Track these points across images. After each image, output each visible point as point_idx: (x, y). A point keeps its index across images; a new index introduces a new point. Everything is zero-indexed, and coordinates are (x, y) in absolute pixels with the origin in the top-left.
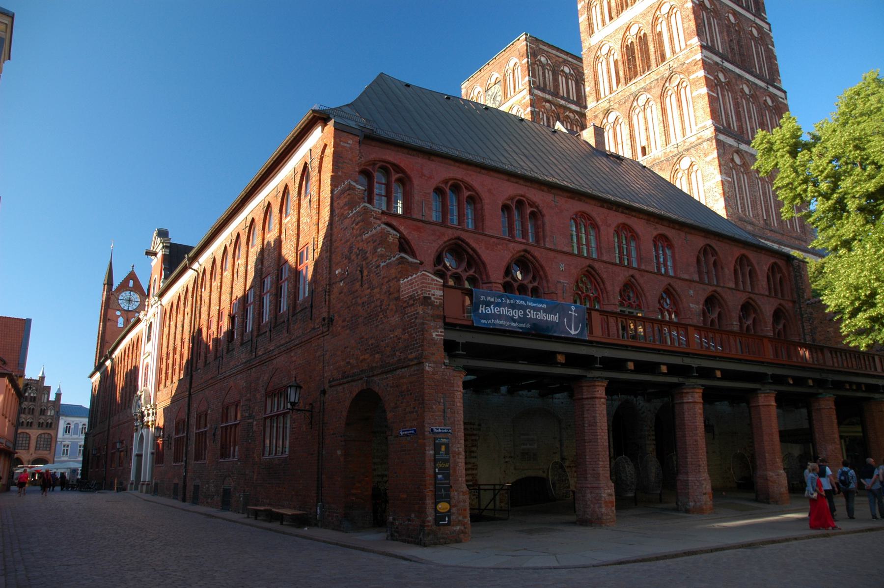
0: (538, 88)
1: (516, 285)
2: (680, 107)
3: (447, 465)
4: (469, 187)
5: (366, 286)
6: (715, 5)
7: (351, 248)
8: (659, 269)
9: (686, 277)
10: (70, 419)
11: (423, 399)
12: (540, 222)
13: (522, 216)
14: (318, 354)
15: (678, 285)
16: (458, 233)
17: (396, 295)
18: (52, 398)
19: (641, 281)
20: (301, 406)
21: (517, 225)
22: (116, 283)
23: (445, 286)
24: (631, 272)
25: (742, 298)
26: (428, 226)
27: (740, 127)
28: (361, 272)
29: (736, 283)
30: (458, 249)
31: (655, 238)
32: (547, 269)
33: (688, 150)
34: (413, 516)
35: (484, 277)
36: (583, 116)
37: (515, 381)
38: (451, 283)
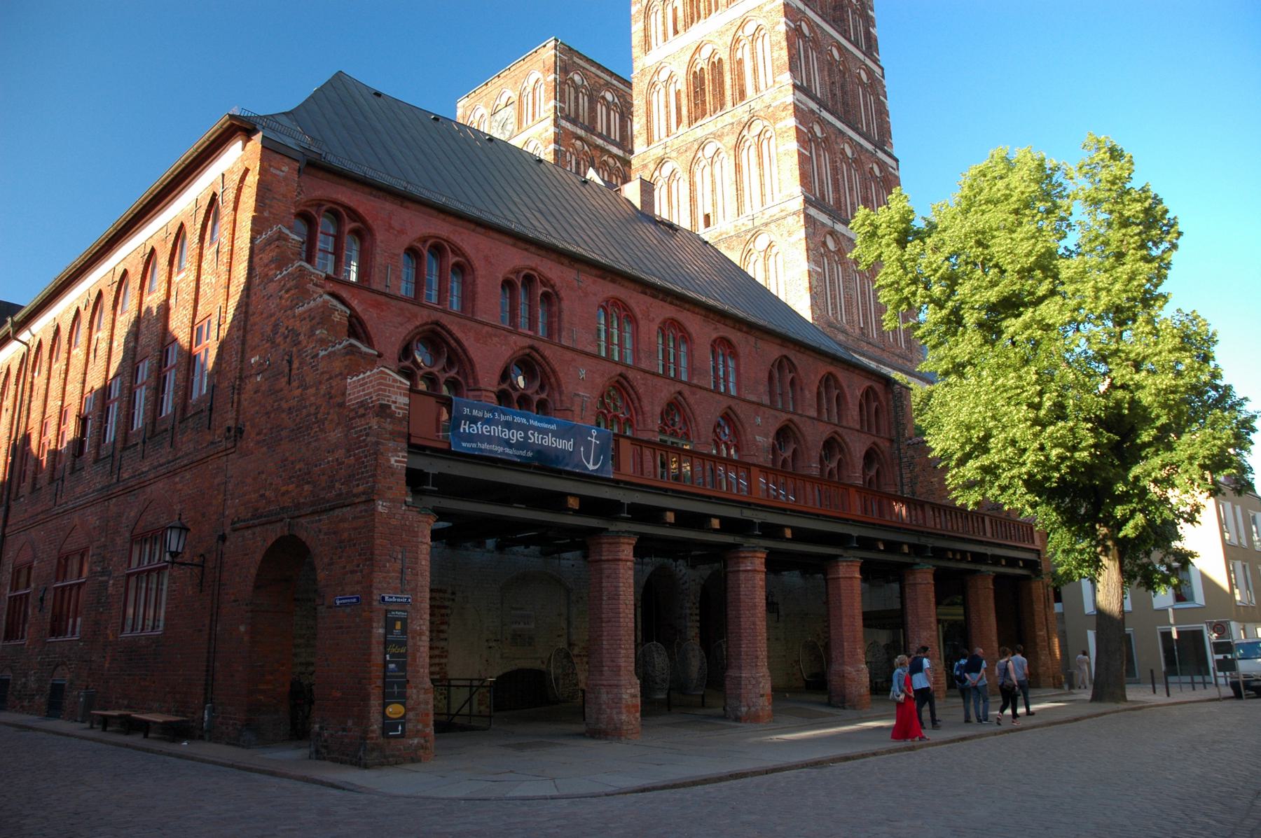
0: (567, 118)
1: (515, 395)
2: (761, 165)
3: (403, 650)
4: (457, 251)
5: (295, 384)
6: (815, 33)
7: (276, 326)
8: (717, 385)
9: (753, 398)
11: (372, 554)
12: (555, 309)
15: (742, 410)
16: (436, 316)
17: (339, 400)
19: (692, 400)
20: (187, 557)
21: (523, 310)
23: (413, 390)
24: (678, 387)
25: (824, 432)
26: (394, 302)
27: (838, 201)
28: (290, 362)
29: (819, 411)
30: (435, 338)
31: (714, 341)
32: (561, 375)
33: (766, 224)
34: (350, 723)
35: (471, 381)
36: (627, 163)
37: (507, 533)
38: (422, 386)
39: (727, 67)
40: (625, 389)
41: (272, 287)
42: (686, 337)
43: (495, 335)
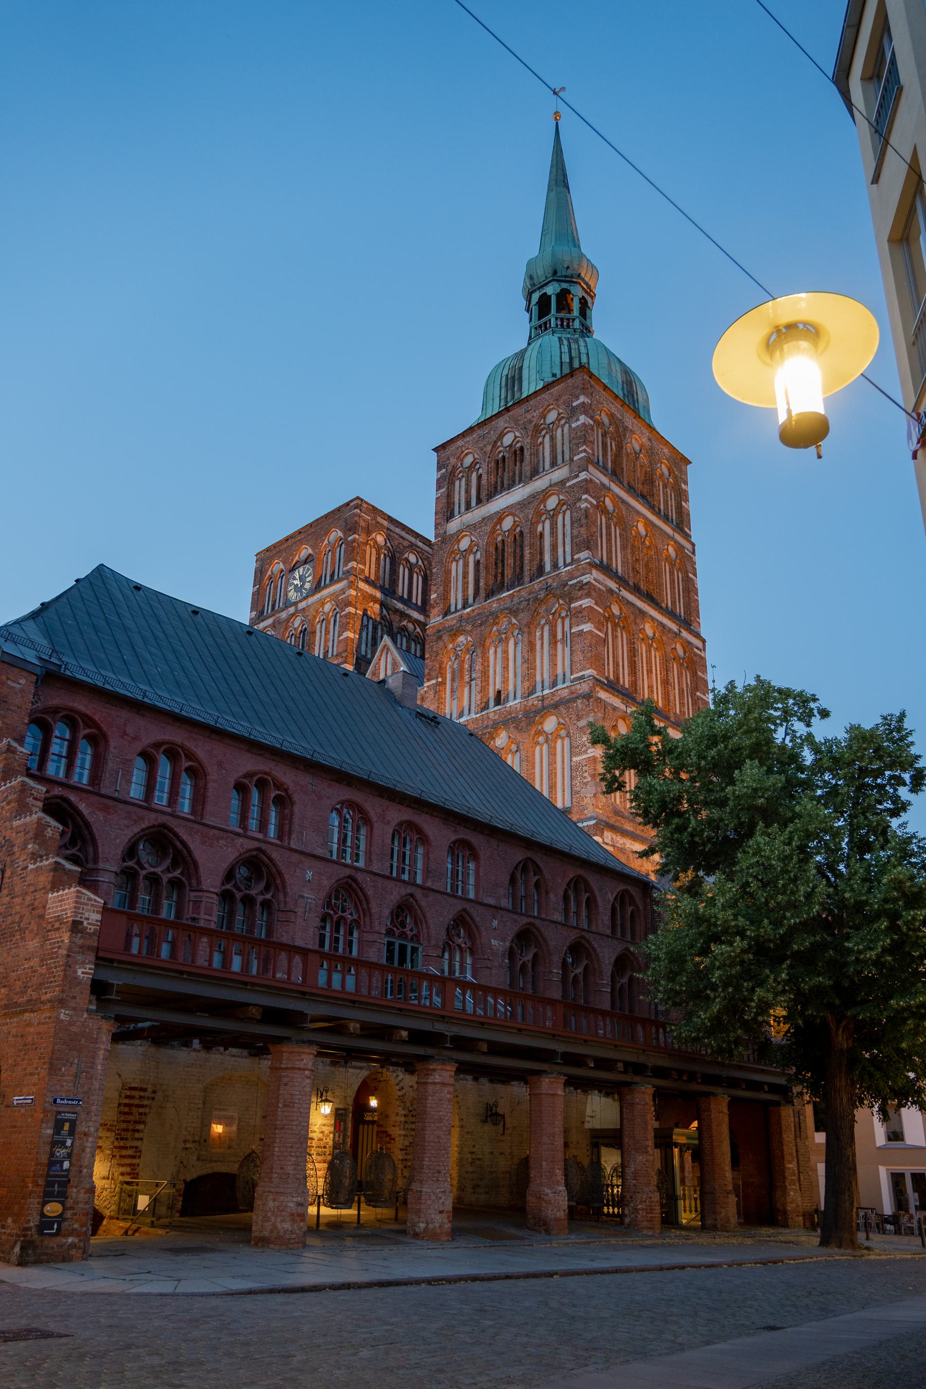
8: (454, 887)
9: (491, 901)
15: (477, 913)
19: (423, 903)
21: (254, 812)
31: (454, 842)
32: (286, 877)
40: (354, 890)
43: (222, 838)
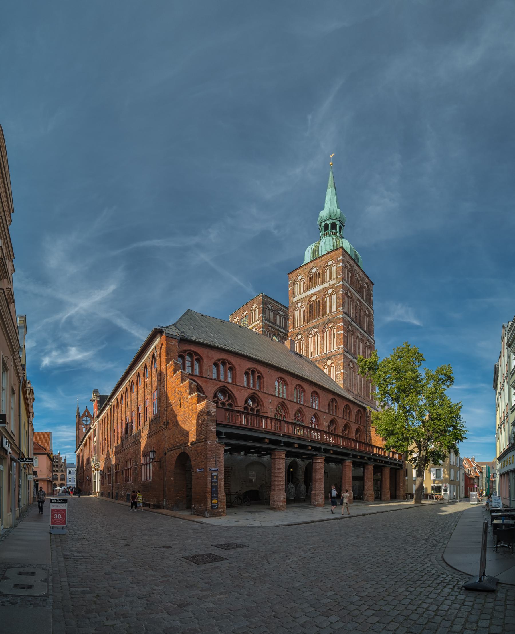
0: (266, 320)
1: (249, 408)
2: (330, 337)
4: (230, 363)
5: (182, 407)
10: (70, 469)
13: (254, 378)
14: (163, 437)
16: (224, 384)
18: (63, 461)
20: (156, 460)
22: (81, 415)
23: (217, 407)
24: (300, 406)
25: (345, 422)
26: (211, 380)
27: (355, 351)
29: (343, 416)
30: (224, 390)
33: (331, 357)
36: (286, 335)
37: (247, 449)
38: (220, 406)
39: (321, 304)
41: (173, 379)
42: (303, 391)
